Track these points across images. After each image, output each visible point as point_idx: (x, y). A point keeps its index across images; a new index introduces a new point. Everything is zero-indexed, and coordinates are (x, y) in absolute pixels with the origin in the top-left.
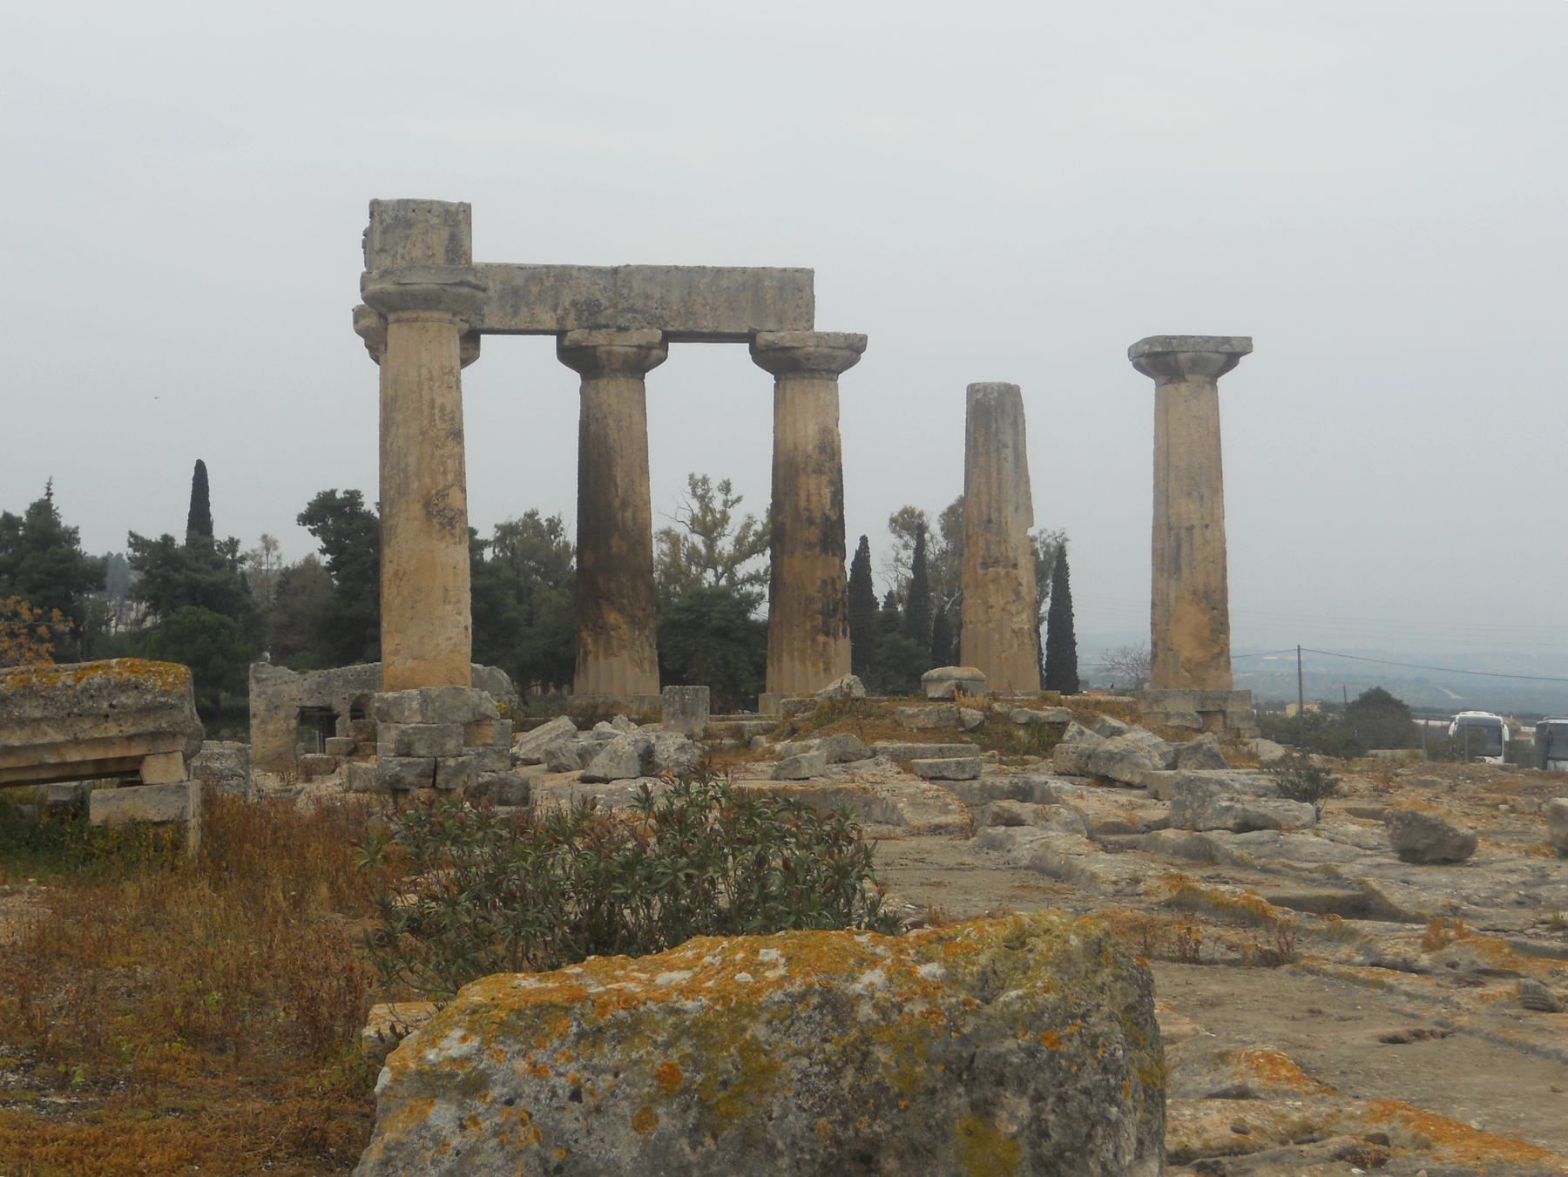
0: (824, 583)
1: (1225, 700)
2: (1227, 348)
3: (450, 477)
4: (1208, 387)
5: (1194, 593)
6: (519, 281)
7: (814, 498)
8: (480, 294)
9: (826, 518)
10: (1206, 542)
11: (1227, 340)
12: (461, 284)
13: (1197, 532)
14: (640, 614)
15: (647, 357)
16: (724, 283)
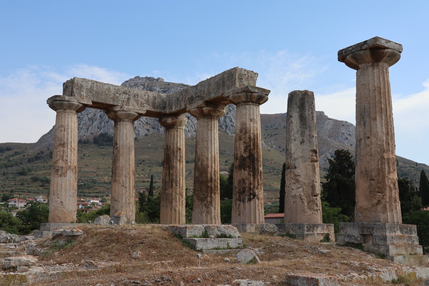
0: (240, 181)
1: (373, 229)
2: (365, 46)
3: (58, 157)
4: (370, 69)
5: (362, 173)
6: (178, 96)
7: (238, 149)
8: (66, 102)
9: (242, 156)
10: (367, 145)
11: (365, 42)
12: (56, 100)
13: (363, 141)
14: (202, 196)
15: (202, 111)
16: (216, 80)
